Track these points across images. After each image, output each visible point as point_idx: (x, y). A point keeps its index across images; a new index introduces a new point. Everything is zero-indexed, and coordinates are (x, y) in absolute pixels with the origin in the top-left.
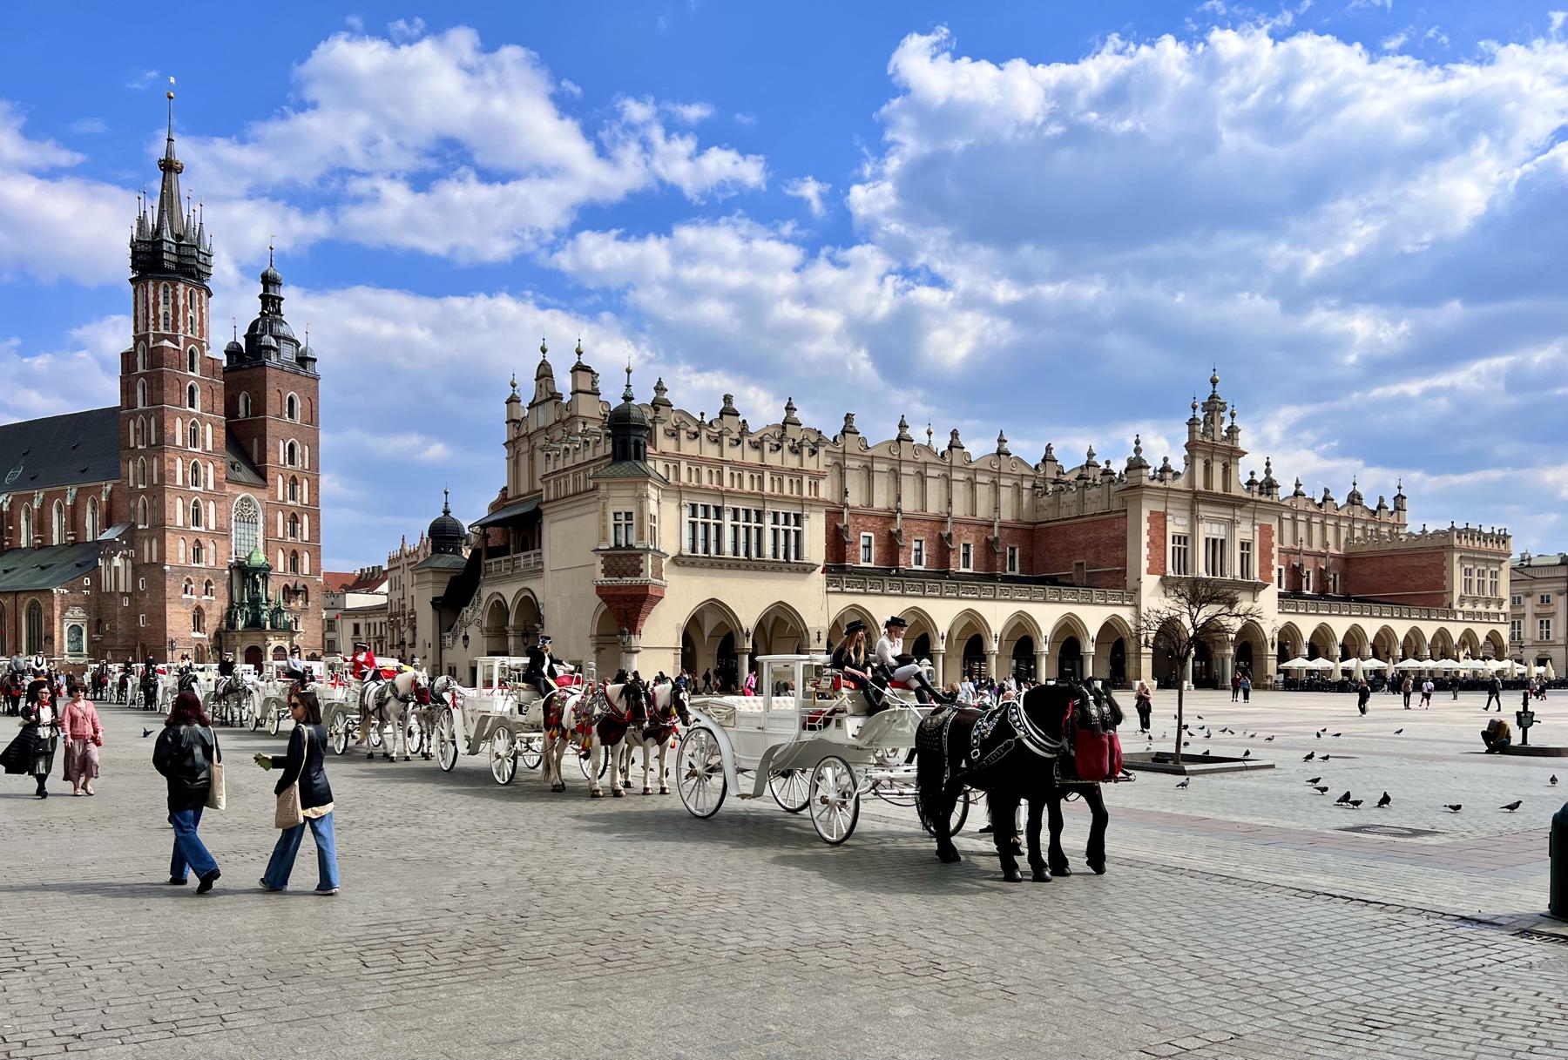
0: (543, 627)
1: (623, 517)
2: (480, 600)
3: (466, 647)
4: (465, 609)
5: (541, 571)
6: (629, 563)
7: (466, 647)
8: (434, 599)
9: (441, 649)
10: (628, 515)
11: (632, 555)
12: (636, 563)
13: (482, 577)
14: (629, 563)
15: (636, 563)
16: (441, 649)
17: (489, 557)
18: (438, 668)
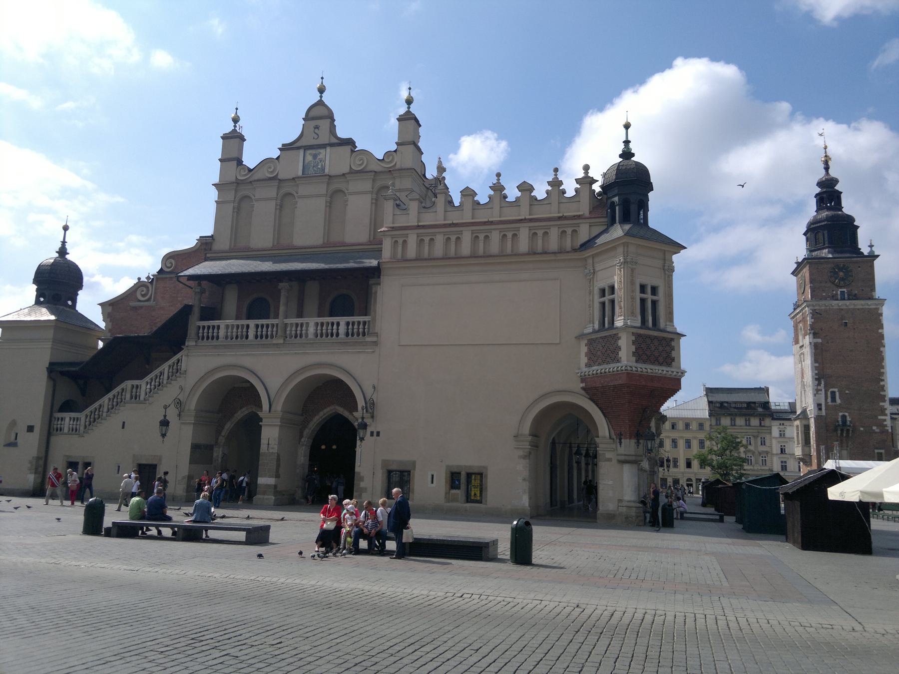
0: (373, 417)
1: (649, 290)
2: (176, 371)
3: (164, 435)
4: (128, 384)
5: (375, 343)
6: (661, 348)
7: (164, 435)
8: (51, 364)
9: (49, 434)
10: (654, 290)
11: (664, 338)
12: (668, 348)
13: (190, 343)
14: (661, 348)
15: (668, 348)
16: (49, 434)
17: (202, 318)
18: (41, 462)
